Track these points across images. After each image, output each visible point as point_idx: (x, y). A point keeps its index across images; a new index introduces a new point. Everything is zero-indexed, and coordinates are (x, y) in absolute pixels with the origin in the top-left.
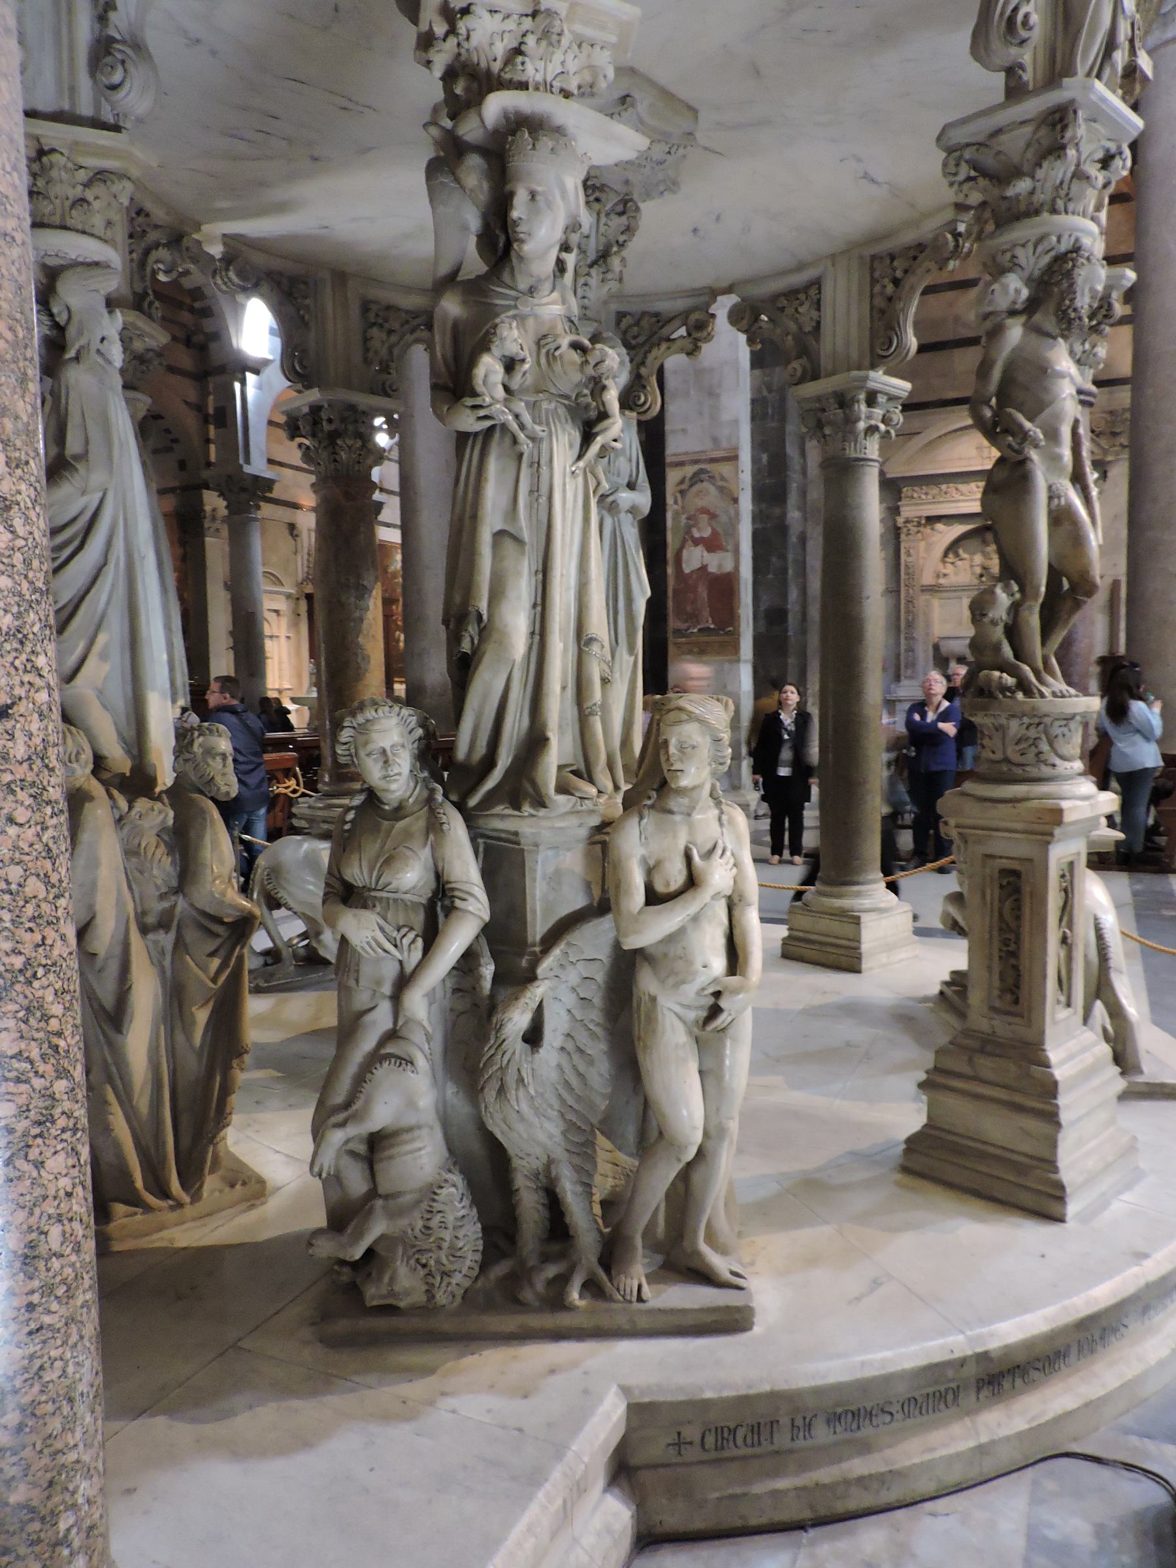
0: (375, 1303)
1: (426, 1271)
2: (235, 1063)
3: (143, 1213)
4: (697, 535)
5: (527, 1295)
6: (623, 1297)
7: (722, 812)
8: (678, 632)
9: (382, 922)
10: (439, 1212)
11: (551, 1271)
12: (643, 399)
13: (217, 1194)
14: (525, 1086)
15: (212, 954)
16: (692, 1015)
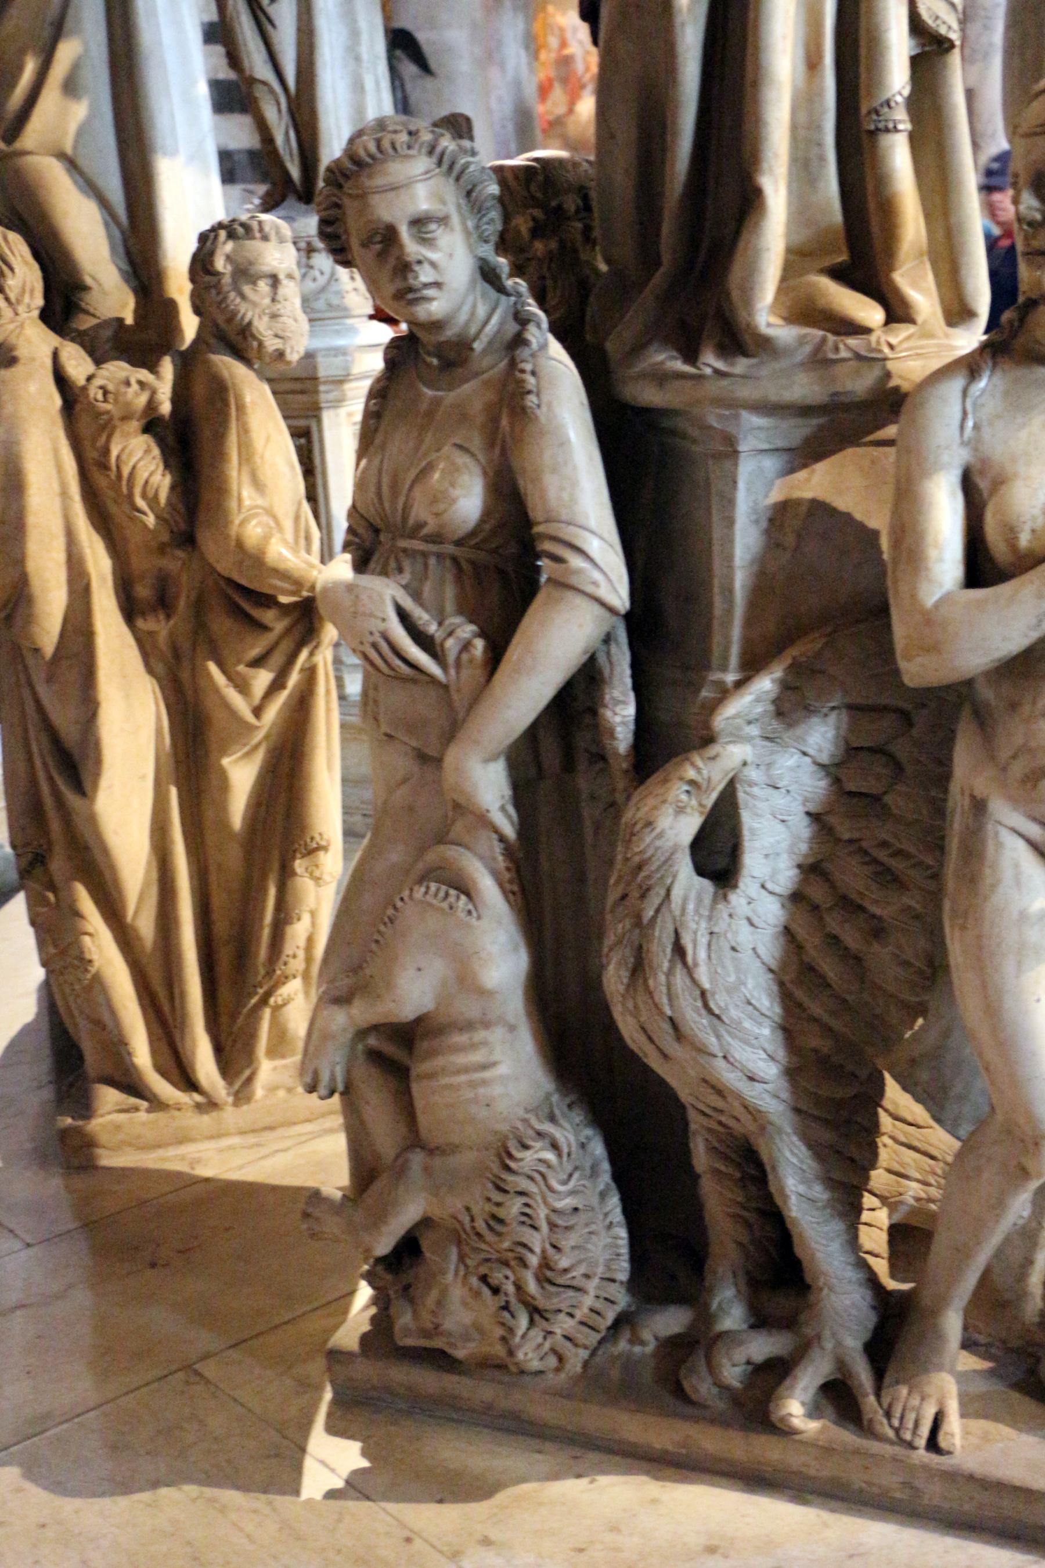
0: (410, 1342)
1: (501, 1300)
2: (299, 865)
3: (149, 1111)
5: (702, 1387)
6: (897, 1431)
10: (522, 1193)
13: (281, 1093)
14: (684, 963)
15: (258, 663)
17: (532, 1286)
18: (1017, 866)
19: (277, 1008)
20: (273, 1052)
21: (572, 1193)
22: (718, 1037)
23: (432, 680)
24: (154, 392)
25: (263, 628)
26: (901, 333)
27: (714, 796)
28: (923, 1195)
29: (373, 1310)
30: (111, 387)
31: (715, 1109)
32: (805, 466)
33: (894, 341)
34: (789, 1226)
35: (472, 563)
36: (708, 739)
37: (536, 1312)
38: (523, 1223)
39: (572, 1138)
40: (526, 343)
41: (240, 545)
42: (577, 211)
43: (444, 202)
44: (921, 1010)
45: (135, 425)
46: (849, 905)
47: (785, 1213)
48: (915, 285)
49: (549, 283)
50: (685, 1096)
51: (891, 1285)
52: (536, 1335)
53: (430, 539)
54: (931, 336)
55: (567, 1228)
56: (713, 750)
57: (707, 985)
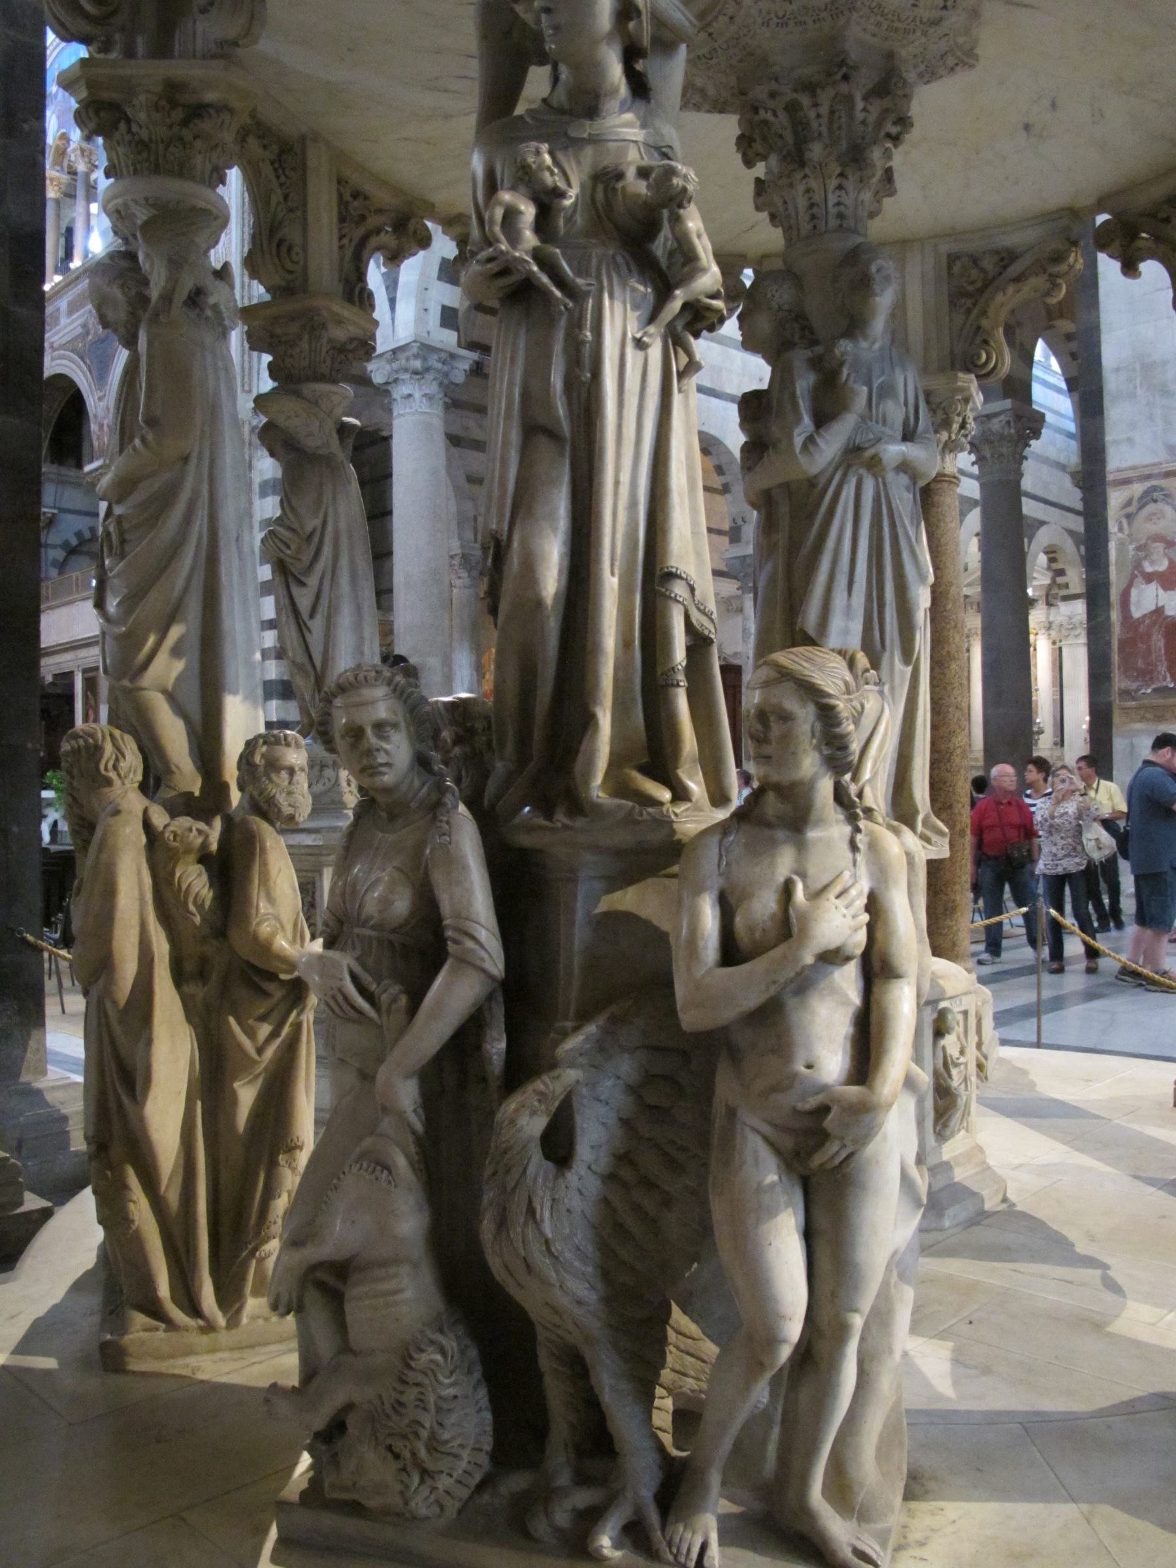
0: (337, 1495)
1: (400, 1464)
2: (282, 1158)
3: (165, 1331)
4: (1148, 568)
5: (540, 1528)
6: (676, 1556)
7: (857, 830)
8: (1126, 694)
9: (358, 969)
10: (417, 1385)
11: (583, 1498)
12: (984, 357)
13: (260, 1321)
14: (535, 1222)
15: (263, 1018)
16: (788, 1143)
17: (423, 1453)
18: (756, 1152)
19: (261, 1260)
20: (256, 1293)
21: (453, 1385)
22: (557, 1272)
23: (370, 1019)
24: (207, 836)
25: (266, 994)
26: (681, 808)
27: (557, 1103)
28: (696, 1387)
29: (311, 1473)
30: (179, 832)
31: (555, 1325)
32: (621, 888)
33: (678, 811)
34: (604, 1409)
35: (404, 946)
36: (554, 1065)
37: (425, 1474)
38: (417, 1406)
39: (455, 1345)
40: (445, 804)
41: (255, 937)
42: (484, 730)
43: (395, 714)
44: (696, 1258)
45: (192, 857)
46: (648, 1184)
47: (601, 1399)
48: (691, 778)
49: (463, 773)
50: (533, 1316)
51: (675, 1453)
52: (425, 1491)
53: (373, 928)
54: (701, 810)
55: (449, 1410)
56: (555, 1073)
57: (550, 1235)
